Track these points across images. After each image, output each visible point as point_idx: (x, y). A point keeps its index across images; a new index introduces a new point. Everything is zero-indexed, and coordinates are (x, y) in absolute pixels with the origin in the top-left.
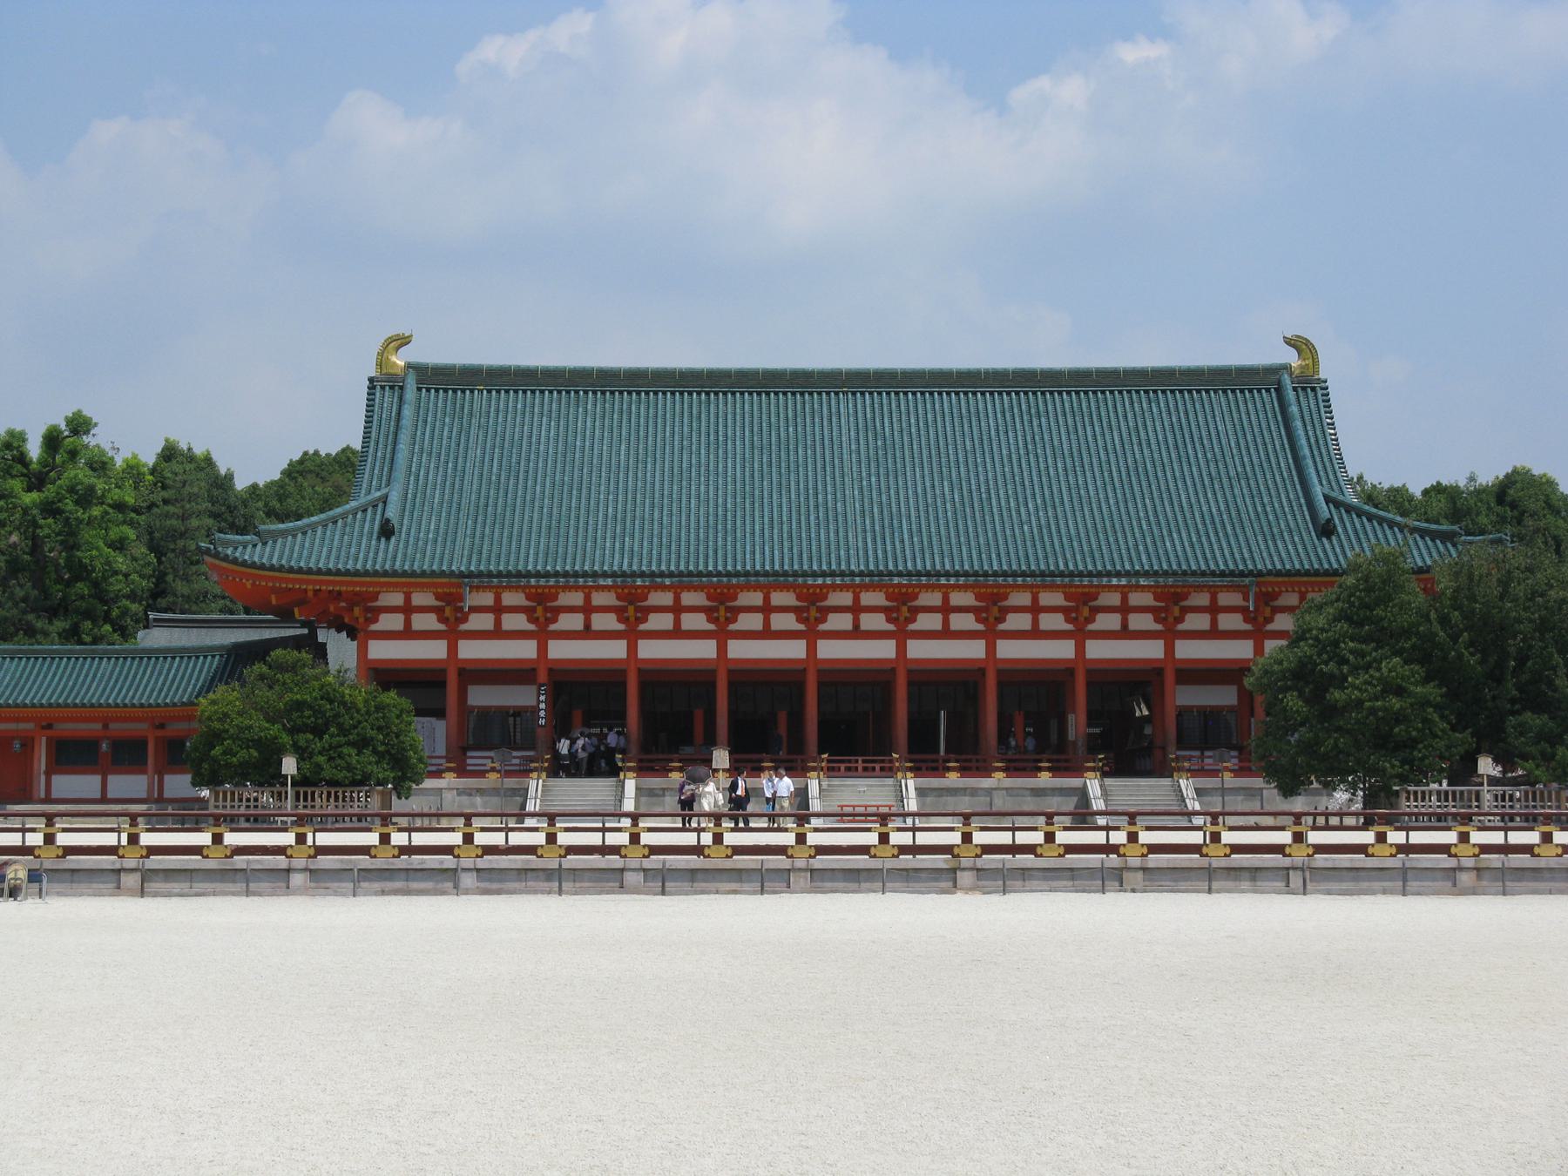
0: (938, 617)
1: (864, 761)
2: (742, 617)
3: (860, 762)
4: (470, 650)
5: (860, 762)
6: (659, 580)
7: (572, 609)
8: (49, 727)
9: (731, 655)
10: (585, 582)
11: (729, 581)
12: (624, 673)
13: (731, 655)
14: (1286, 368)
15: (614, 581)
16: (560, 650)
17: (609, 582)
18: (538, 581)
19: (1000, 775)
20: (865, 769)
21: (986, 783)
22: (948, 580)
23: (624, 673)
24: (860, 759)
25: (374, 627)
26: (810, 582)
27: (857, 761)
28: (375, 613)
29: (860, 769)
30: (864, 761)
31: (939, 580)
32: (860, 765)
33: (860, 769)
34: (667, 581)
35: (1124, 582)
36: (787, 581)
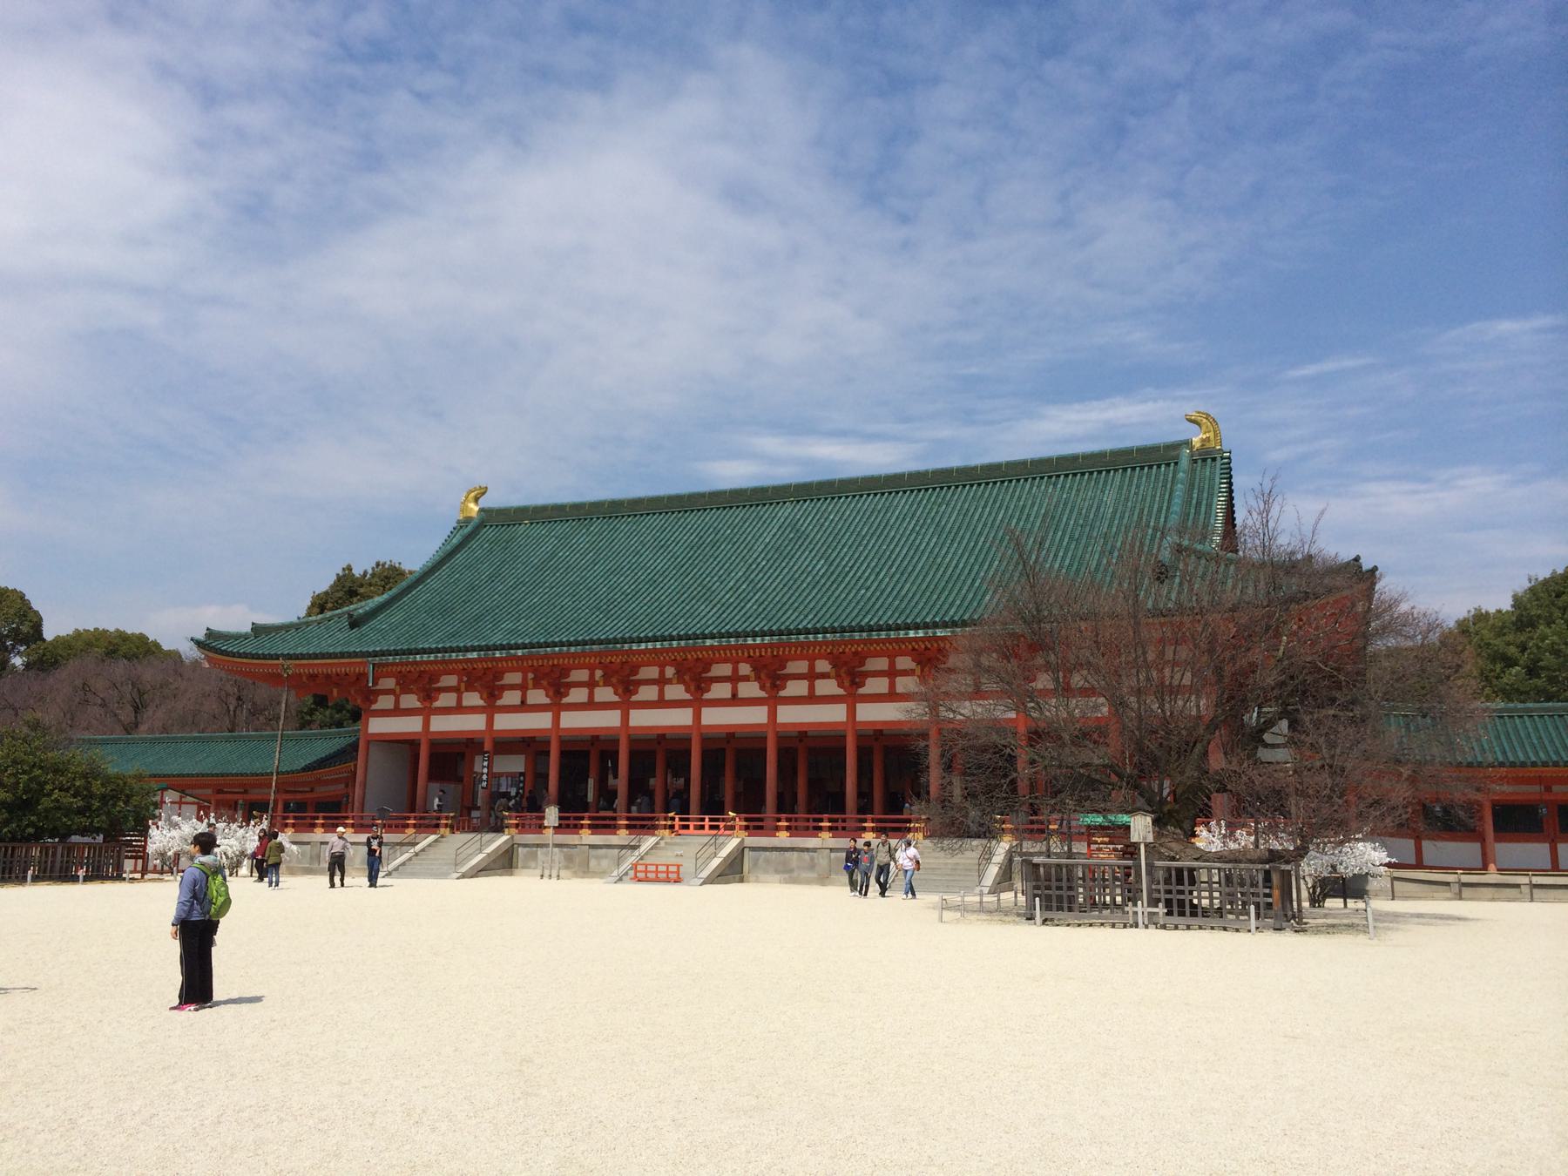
0: (805, 684)
1: (711, 820)
2: (642, 689)
3: (707, 820)
4: (440, 724)
5: (707, 820)
6: (512, 651)
7: (512, 687)
8: (246, 792)
9: (632, 723)
10: (457, 656)
11: (569, 650)
12: (616, 742)
13: (632, 723)
14: (1188, 443)
15: (478, 655)
16: (504, 722)
17: (475, 655)
18: (422, 657)
19: (826, 835)
20: (712, 827)
21: (811, 842)
22: (754, 640)
23: (615, 742)
24: (707, 817)
25: (374, 707)
26: (634, 648)
27: (703, 820)
28: (371, 695)
29: (707, 827)
30: (711, 820)
31: (746, 641)
32: (707, 823)
33: (707, 827)
34: (520, 652)
35: (921, 634)
36: (616, 647)
